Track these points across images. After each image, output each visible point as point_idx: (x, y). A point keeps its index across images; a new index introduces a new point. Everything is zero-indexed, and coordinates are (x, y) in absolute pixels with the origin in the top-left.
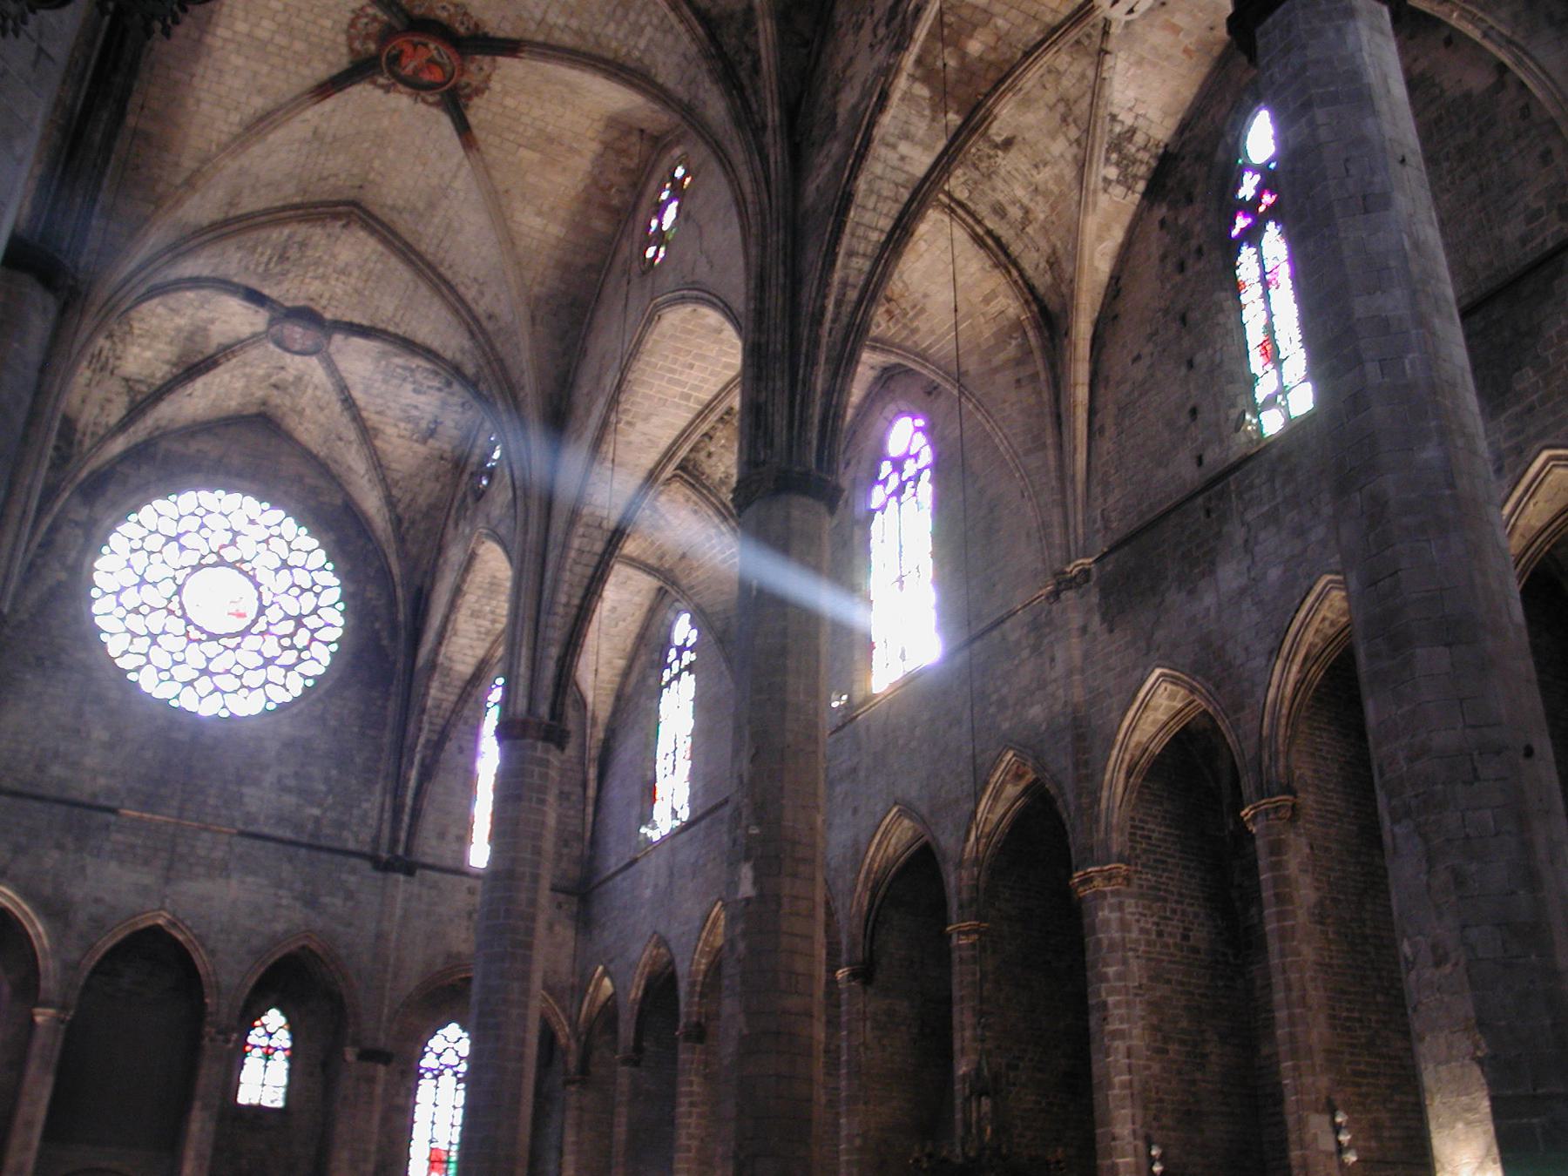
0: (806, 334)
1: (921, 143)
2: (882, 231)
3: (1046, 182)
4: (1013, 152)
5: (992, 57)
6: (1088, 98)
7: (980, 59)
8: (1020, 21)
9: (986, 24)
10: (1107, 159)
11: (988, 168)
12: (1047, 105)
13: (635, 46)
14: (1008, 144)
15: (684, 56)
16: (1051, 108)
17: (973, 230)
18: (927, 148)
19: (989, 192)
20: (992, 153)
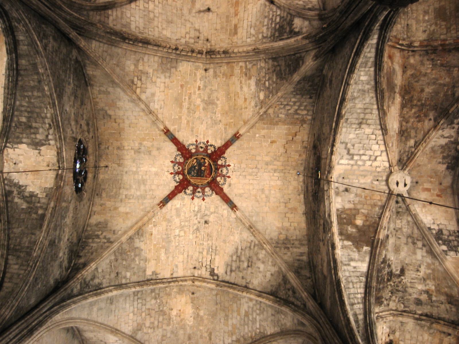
0: (346, 331)
1: (359, 260)
2: (361, 293)
3: (425, 273)
4: (407, 273)
5: (368, 223)
6: (415, 228)
7: (364, 225)
8: (370, 208)
9: (358, 214)
10: (439, 244)
11: (402, 287)
12: (405, 244)
13: (257, 328)
14: (402, 271)
15: (272, 315)
16: (407, 244)
17: (413, 317)
18: (363, 261)
19: (410, 297)
20: (400, 280)
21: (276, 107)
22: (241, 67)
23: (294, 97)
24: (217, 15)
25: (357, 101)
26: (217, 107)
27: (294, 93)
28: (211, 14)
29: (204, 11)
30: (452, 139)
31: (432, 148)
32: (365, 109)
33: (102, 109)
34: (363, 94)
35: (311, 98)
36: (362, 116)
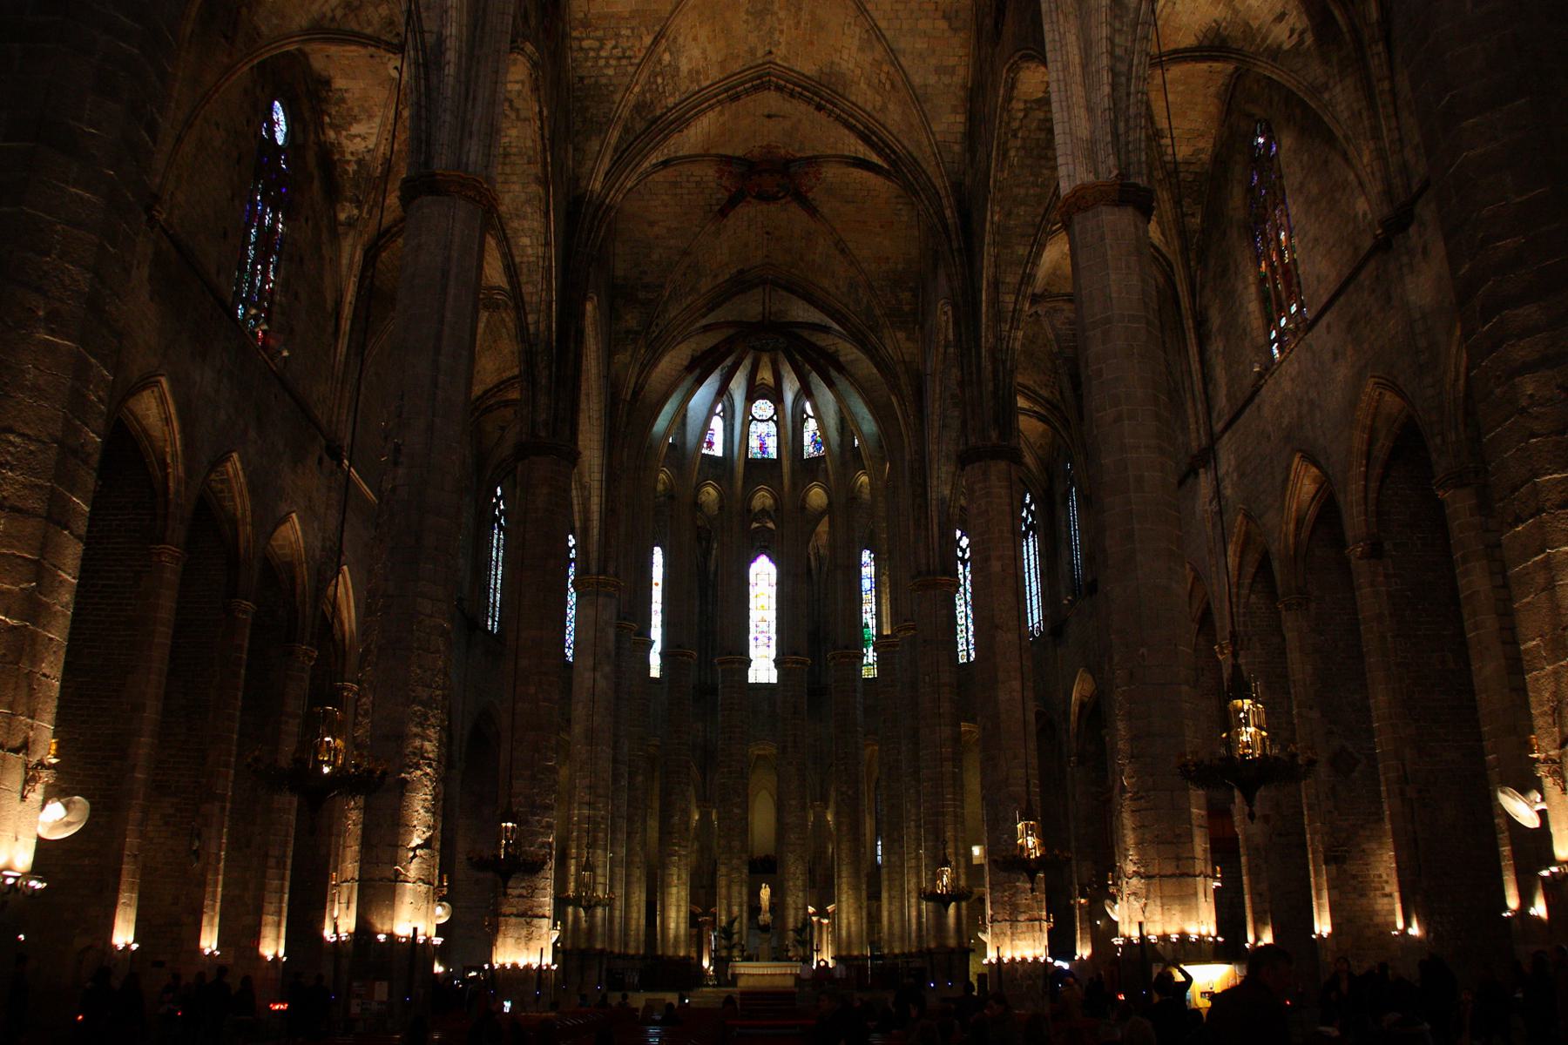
6: (356, 28)
21: (639, 50)
22: (708, 79)
23: (610, 78)
24: (754, 115)
25: (523, 196)
26: (747, 9)
27: (611, 88)
28: (766, 113)
29: (778, 116)
30: (344, 133)
31: (371, 117)
32: (505, 182)
33: (955, 30)
34: (516, 209)
35: (582, 79)
36: (508, 170)
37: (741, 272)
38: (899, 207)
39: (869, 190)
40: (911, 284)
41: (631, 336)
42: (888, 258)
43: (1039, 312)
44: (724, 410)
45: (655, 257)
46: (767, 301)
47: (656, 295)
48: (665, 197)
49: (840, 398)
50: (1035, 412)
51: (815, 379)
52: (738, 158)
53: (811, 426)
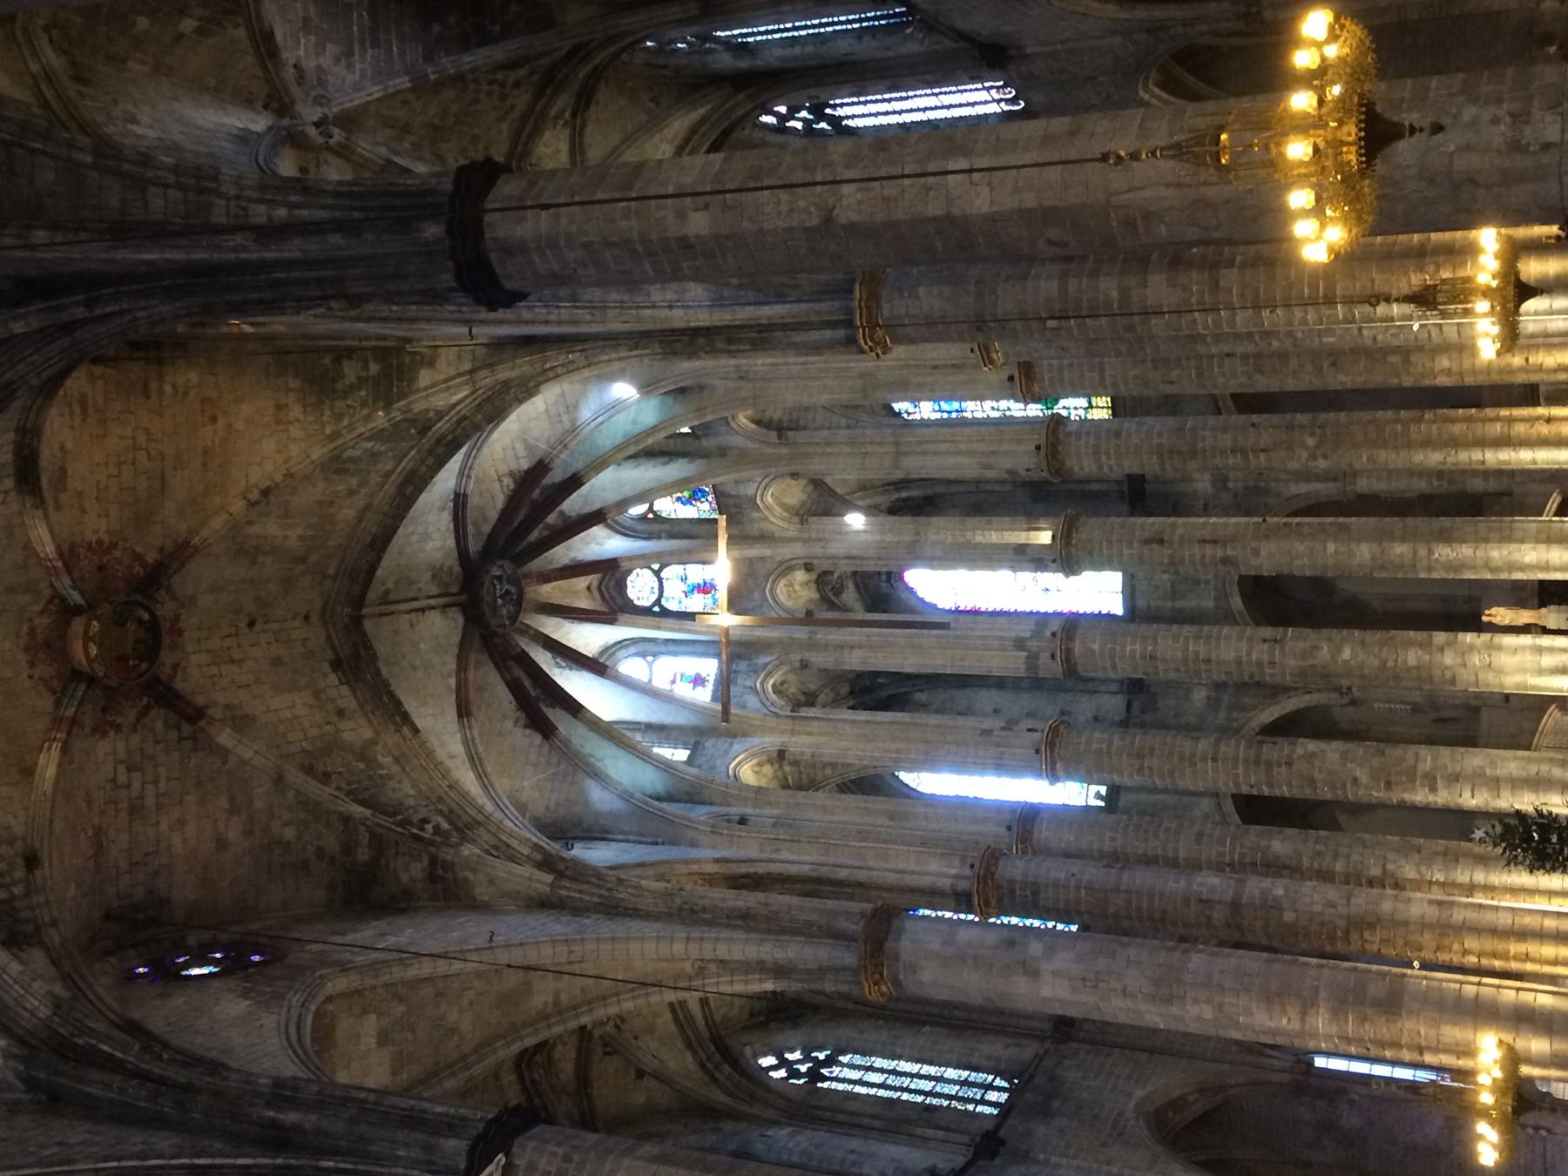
37: (336, 665)
38: (168, 388)
39: (136, 448)
40: (327, 360)
41: (440, 872)
42: (279, 407)
43: (316, 119)
44: (643, 655)
45: (289, 833)
46: (403, 606)
47: (362, 828)
48: (164, 826)
49: (600, 464)
50: (574, 115)
51: (573, 505)
52: (58, 703)
53: (667, 506)
